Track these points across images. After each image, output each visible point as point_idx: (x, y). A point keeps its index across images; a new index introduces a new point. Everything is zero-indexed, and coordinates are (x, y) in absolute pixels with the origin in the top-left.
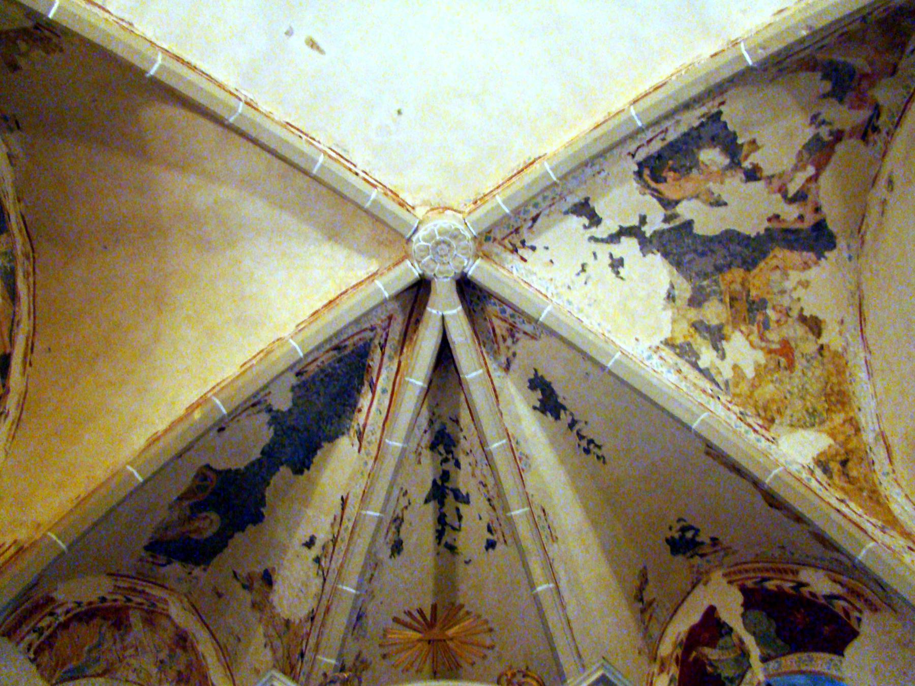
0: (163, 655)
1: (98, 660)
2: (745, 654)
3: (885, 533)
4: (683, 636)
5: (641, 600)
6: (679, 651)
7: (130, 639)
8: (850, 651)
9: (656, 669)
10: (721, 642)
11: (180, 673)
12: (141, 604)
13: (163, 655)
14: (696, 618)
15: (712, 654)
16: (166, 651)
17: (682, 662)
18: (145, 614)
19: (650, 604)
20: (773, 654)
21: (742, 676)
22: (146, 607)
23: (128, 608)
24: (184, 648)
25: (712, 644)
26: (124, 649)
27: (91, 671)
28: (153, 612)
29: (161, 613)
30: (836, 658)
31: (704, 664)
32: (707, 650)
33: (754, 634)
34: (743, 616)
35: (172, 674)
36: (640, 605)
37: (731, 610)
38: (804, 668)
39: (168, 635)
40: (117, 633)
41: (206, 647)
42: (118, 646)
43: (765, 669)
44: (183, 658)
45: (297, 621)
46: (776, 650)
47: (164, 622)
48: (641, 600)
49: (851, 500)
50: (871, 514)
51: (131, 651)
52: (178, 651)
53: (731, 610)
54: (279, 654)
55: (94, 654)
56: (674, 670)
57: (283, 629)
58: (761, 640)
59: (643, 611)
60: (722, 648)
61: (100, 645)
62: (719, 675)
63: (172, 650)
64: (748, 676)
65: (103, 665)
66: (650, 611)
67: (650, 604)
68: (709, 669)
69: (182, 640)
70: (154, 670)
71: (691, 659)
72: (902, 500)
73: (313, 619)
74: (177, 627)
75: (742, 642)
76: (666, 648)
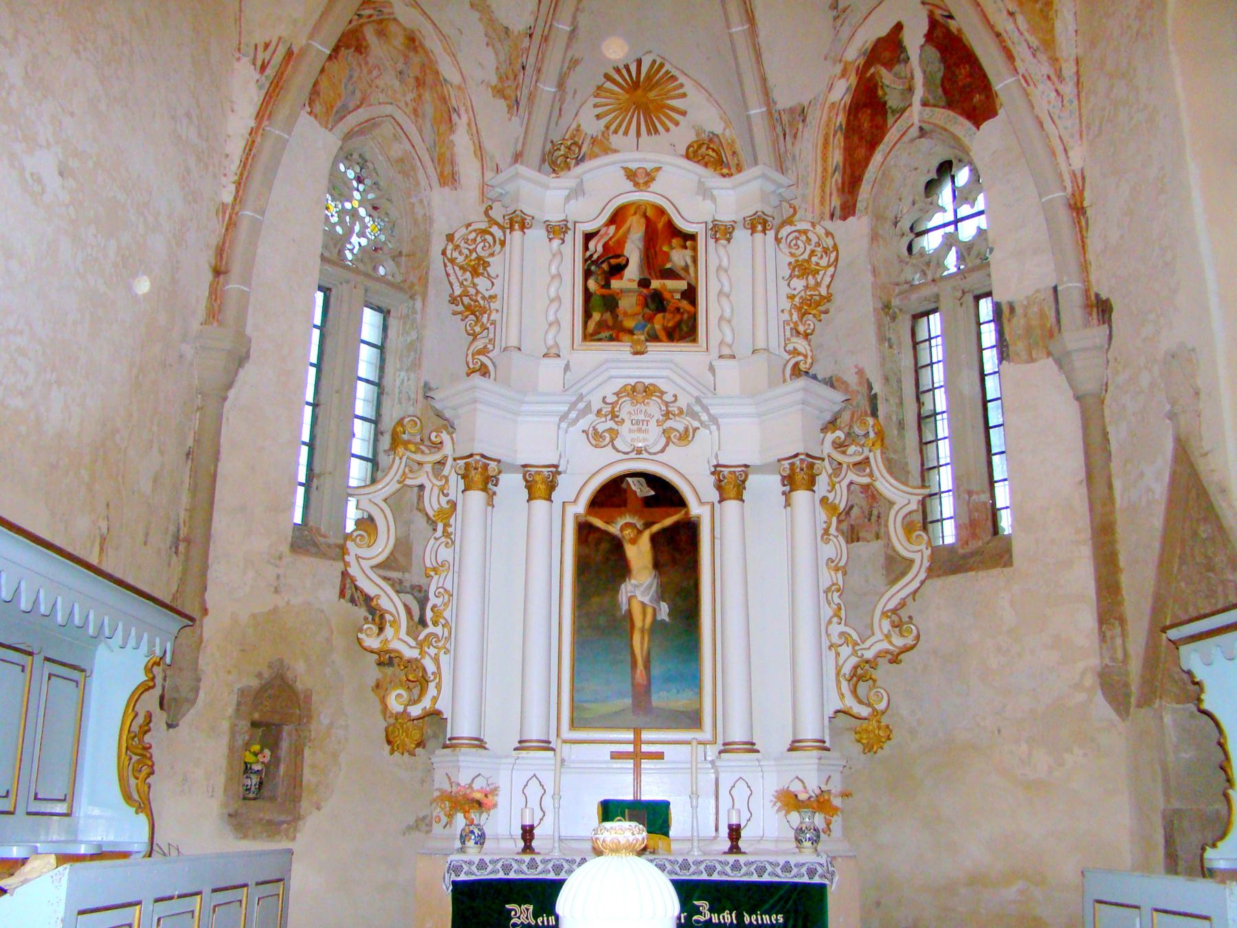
0: (400, 66)
1: (353, 93)
2: (911, 90)
3: (1034, 56)
4: (869, 45)
5: (836, 8)
6: (861, 61)
7: (371, 61)
8: (986, 126)
9: (838, 68)
10: (897, 68)
11: (417, 79)
12: (370, 16)
13: (400, 66)
14: (883, 31)
15: (886, 76)
16: (402, 60)
17: (861, 72)
18: (375, 26)
19: (844, 11)
20: (932, 101)
21: (903, 111)
22: (375, 18)
23: (361, 25)
24: (415, 49)
25: (889, 65)
26: (370, 72)
27: (351, 107)
28: (381, 21)
29: (388, 19)
30: (974, 129)
31: (876, 85)
32: (883, 71)
33: (924, 72)
34: (922, 47)
35: (412, 81)
36: (835, 13)
37: (914, 39)
38: (948, 127)
39: (399, 41)
40: (361, 57)
41: (432, 43)
42: (365, 71)
43: (921, 113)
44: (416, 59)
45: (516, 33)
46: (935, 98)
47: (393, 27)
48: (836, 8)
49: (1022, 13)
50: (1033, 30)
51: (375, 73)
52: (411, 54)
53: (914, 39)
54: (502, 58)
55: (350, 88)
56: (853, 79)
57: (503, 35)
58: (928, 82)
59: (836, 18)
60: (896, 75)
61: (351, 77)
62: (885, 103)
63: (406, 57)
64: (906, 114)
65: (358, 95)
66: (843, 16)
67: (844, 11)
68: (880, 93)
69: (412, 41)
70: (397, 84)
71: (868, 75)
72: (1070, 18)
73: (531, 36)
74: (405, 29)
75: (912, 78)
76: (854, 53)
